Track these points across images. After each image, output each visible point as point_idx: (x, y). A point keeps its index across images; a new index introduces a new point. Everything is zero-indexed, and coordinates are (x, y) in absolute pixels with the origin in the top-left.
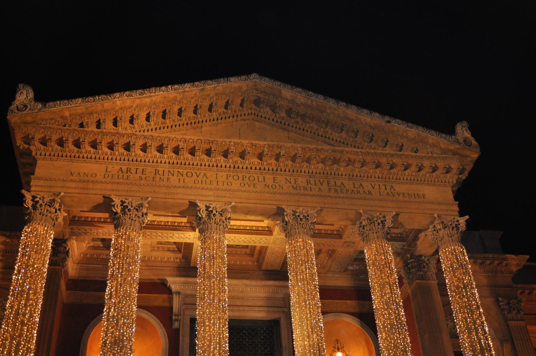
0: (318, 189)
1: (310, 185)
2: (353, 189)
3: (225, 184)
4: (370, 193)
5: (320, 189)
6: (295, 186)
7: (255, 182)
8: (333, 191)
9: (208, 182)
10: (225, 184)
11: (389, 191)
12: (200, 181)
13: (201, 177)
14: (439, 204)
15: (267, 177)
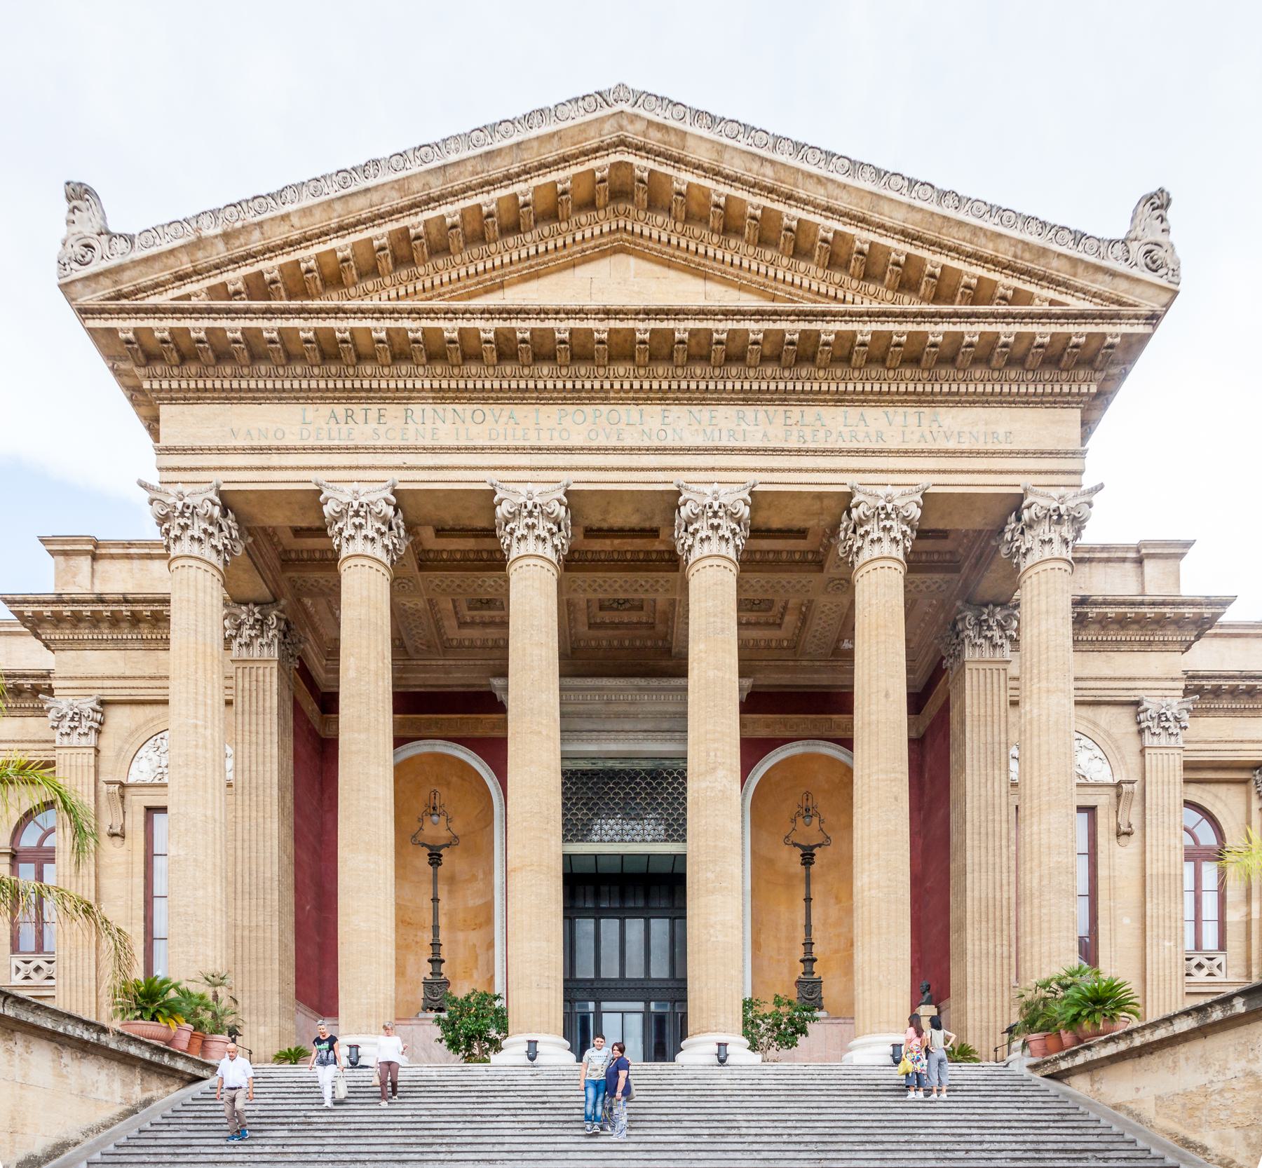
0: (760, 435)
1: (744, 426)
2: (841, 428)
3: (556, 434)
4: (880, 436)
5: (765, 435)
6: (709, 430)
7: (621, 426)
8: (795, 434)
9: (519, 433)
10: (556, 434)
11: (925, 428)
12: (502, 431)
13: (503, 420)
14: (1041, 454)
15: (648, 409)
